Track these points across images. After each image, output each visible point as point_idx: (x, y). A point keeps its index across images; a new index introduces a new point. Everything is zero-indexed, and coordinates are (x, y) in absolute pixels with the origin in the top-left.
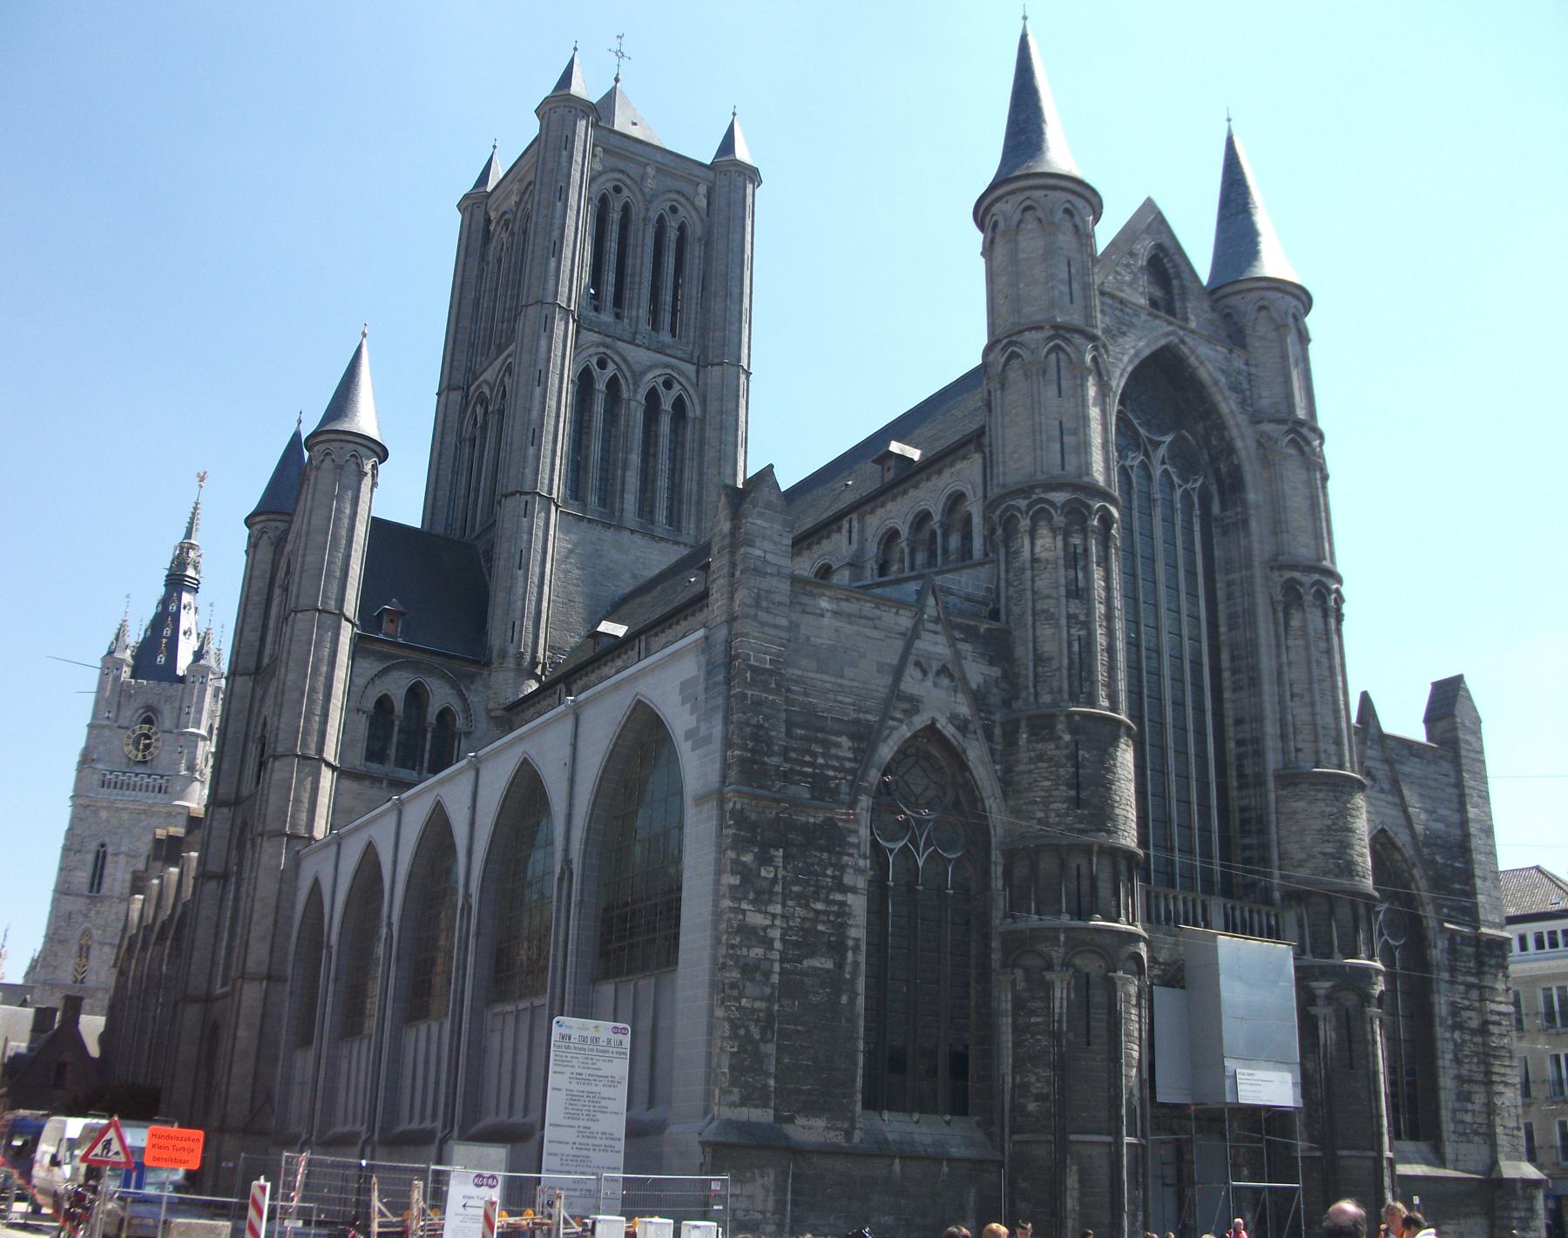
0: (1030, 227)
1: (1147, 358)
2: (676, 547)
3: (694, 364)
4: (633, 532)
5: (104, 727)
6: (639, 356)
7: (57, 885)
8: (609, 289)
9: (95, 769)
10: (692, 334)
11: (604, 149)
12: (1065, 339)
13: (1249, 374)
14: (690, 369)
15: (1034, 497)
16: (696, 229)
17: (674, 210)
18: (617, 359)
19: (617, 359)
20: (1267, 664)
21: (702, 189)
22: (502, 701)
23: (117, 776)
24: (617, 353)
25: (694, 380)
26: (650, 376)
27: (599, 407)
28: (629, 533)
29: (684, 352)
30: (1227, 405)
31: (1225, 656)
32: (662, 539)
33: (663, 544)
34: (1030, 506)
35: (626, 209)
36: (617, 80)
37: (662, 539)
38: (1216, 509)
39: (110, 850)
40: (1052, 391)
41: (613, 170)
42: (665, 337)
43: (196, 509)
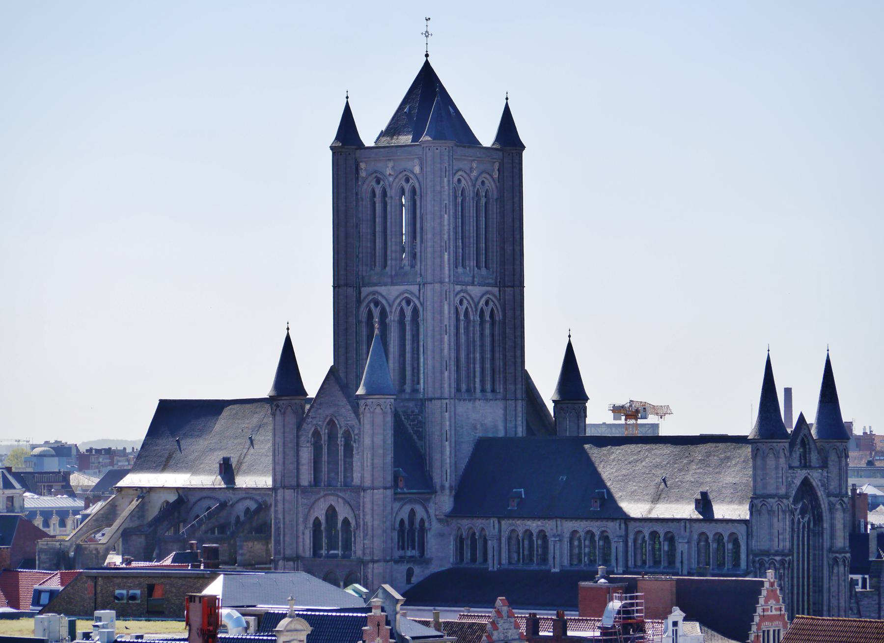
0: (771, 456)
2: (496, 402)
3: (497, 287)
4: (479, 400)
10: (495, 266)
12: (781, 501)
13: (828, 476)
15: (770, 558)
18: (468, 298)
19: (468, 298)
20: (826, 586)
22: (444, 512)
25: (498, 297)
28: (478, 401)
31: (811, 580)
32: (490, 400)
33: (491, 402)
34: (769, 560)
36: (427, 55)
37: (490, 400)
38: (812, 525)
40: (776, 520)
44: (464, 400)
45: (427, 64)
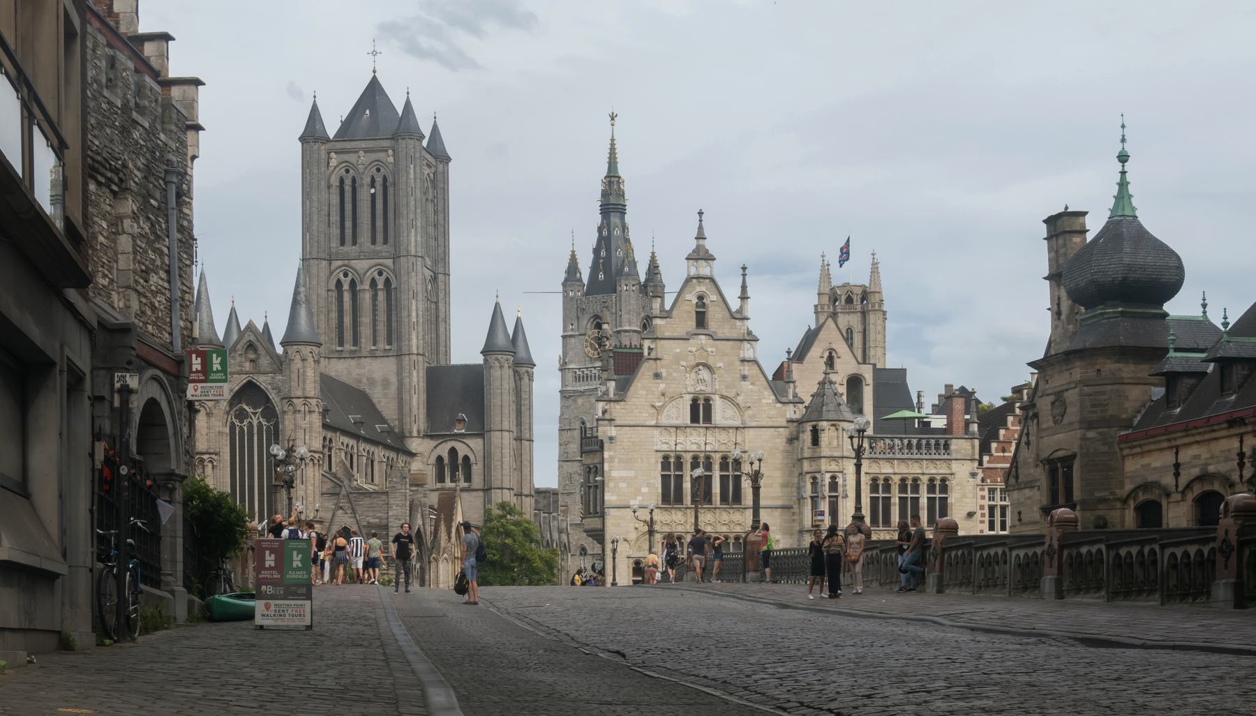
1: (238, 391)
4: (366, 357)
5: (571, 336)
6: (361, 265)
7: (560, 456)
8: (348, 231)
9: (569, 369)
11: (336, 153)
14: (389, 262)
16: (390, 179)
17: (378, 170)
21: (390, 152)
23: (583, 372)
24: (350, 267)
26: (370, 272)
27: (347, 297)
29: (387, 252)
30: (273, 396)
35: (354, 180)
36: (374, 72)
39: (588, 425)
41: (340, 164)
42: (379, 247)
43: (613, 140)
44: (345, 358)
45: (374, 78)
